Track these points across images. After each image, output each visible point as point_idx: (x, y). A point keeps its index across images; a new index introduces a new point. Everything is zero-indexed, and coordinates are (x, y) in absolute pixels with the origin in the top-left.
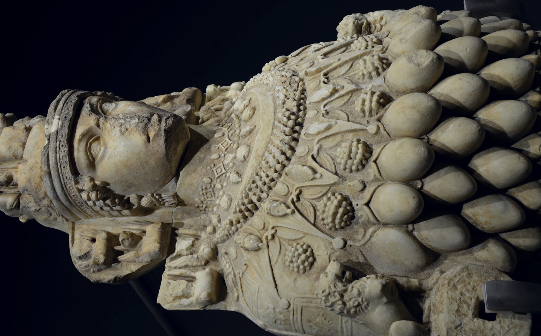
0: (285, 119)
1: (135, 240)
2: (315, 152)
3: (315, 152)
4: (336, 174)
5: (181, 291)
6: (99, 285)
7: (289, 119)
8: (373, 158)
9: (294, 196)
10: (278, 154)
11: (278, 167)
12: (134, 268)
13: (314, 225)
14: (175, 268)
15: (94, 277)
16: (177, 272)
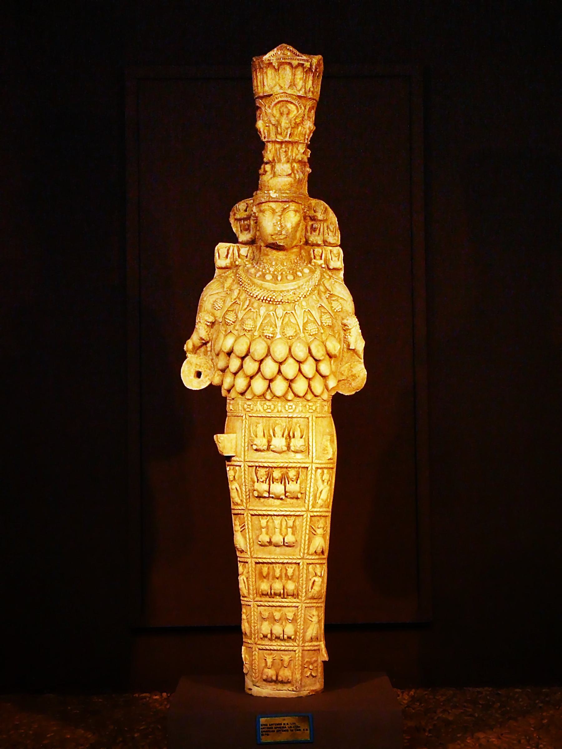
0: (270, 297)
1: (248, 229)
2: (252, 310)
3: (252, 310)
4: (242, 319)
5: (223, 253)
6: (229, 216)
7: (271, 298)
8: (246, 333)
9: (238, 302)
10: (257, 294)
11: (252, 295)
12: (234, 230)
13: (228, 311)
14: (233, 250)
15: (231, 214)
16: (231, 251)
